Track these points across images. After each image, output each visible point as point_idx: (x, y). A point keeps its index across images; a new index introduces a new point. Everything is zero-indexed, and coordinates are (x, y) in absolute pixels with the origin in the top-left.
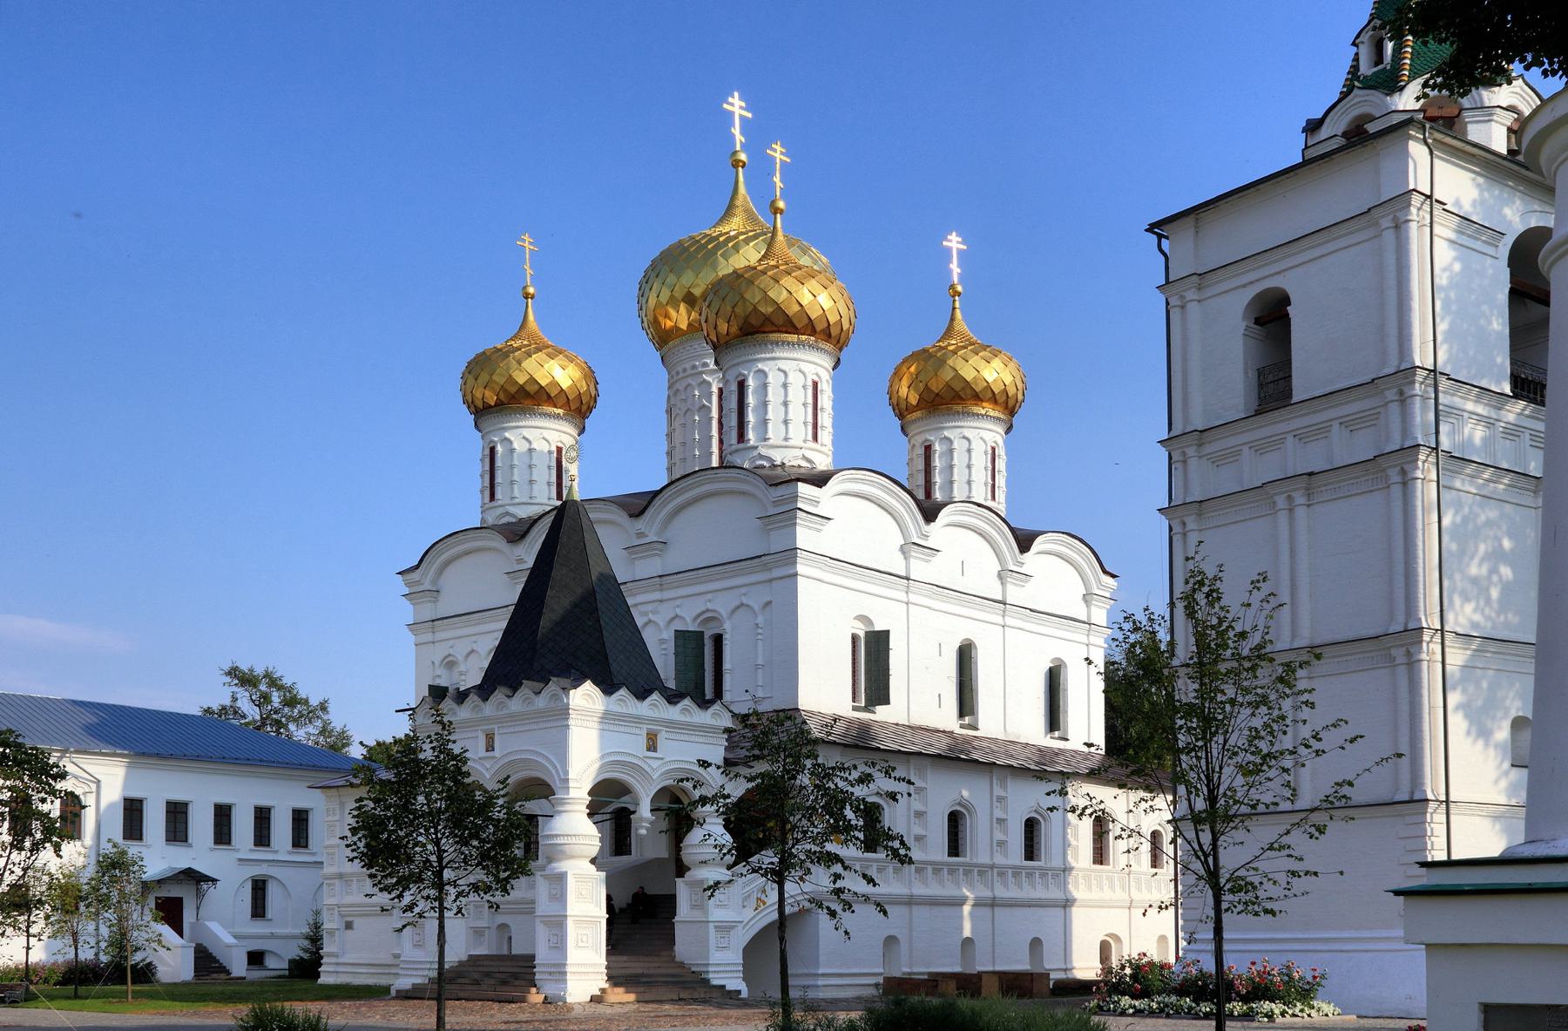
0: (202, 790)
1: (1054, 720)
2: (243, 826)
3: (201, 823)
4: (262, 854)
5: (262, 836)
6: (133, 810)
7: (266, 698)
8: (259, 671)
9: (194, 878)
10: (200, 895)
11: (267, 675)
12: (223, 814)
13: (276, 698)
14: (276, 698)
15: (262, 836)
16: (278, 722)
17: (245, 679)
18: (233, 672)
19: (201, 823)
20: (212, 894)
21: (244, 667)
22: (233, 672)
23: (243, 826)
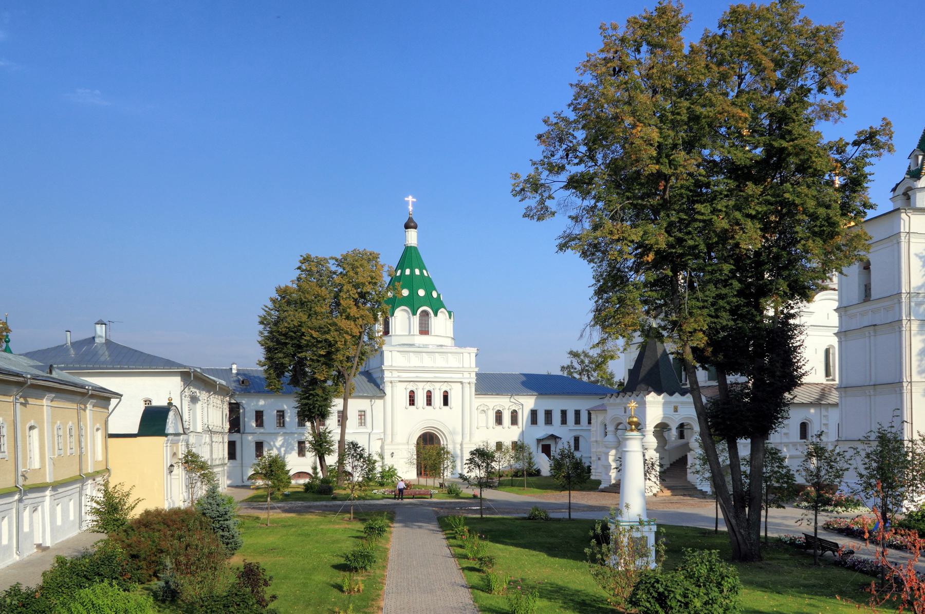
0: (556, 405)
1: (828, 374)
2: (571, 417)
3: (557, 417)
4: (578, 427)
5: (577, 421)
6: (534, 413)
7: (582, 362)
8: (580, 351)
9: (553, 437)
10: (556, 443)
11: (584, 352)
12: (564, 413)
13: (587, 361)
14: (587, 361)
15: (577, 421)
16: (587, 371)
17: (575, 355)
18: (571, 353)
19: (557, 417)
21: (575, 350)
22: (571, 353)
23: (571, 417)
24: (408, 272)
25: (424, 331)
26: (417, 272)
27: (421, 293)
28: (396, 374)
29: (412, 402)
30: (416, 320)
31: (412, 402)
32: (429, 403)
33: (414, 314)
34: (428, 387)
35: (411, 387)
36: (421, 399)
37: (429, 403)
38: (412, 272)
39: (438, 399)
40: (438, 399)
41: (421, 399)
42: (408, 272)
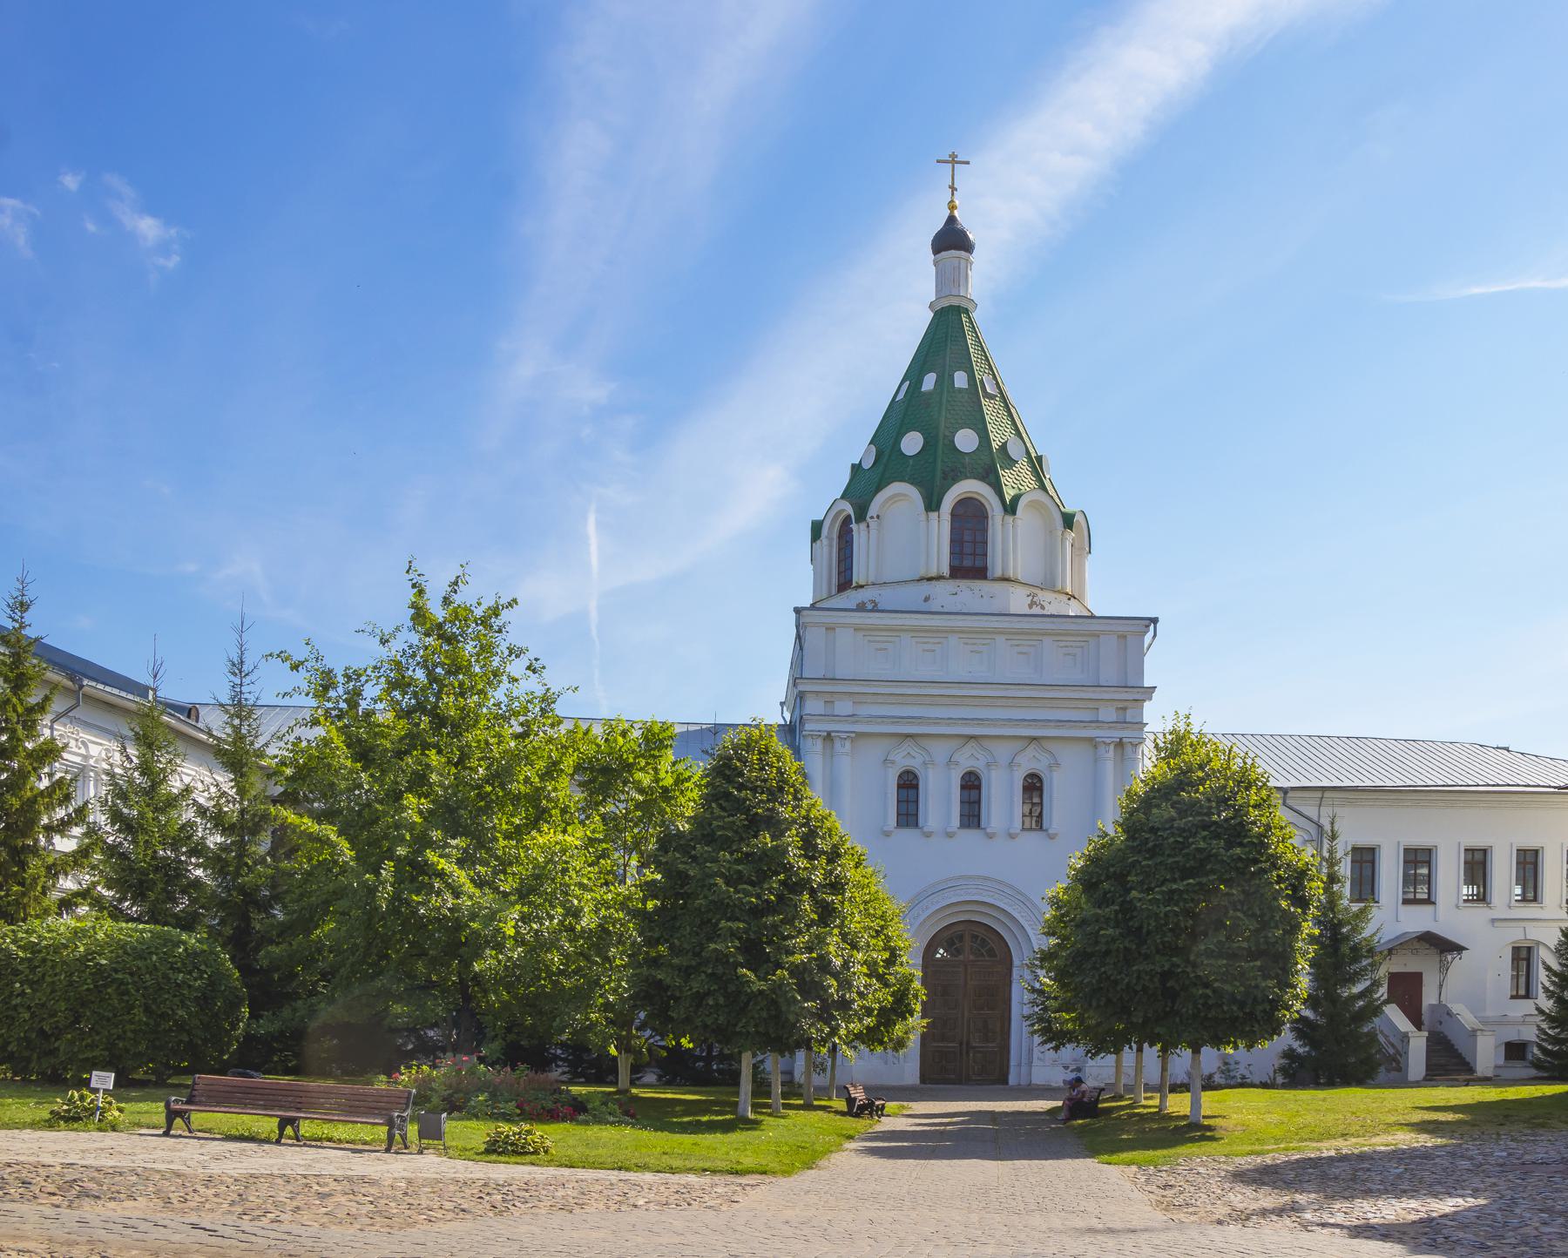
10: (1444, 968)
20: (1459, 966)
24: (929, 382)
25: (970, 561)
26: (960, 379)
27: (966, 440)
28: (843, 707)
29: (908, 814)
30: (941, 526)
31: (908, 814)
32: (972, 815)
33: (932, 505)
34: (968, 759)
35: (906, 757)
36: (940, 799)
37: (972, 815)
38: (945, 381)
39: (1003, 801)
40: (1003, 801)
41: (940, 799)
42: (929, 382)
